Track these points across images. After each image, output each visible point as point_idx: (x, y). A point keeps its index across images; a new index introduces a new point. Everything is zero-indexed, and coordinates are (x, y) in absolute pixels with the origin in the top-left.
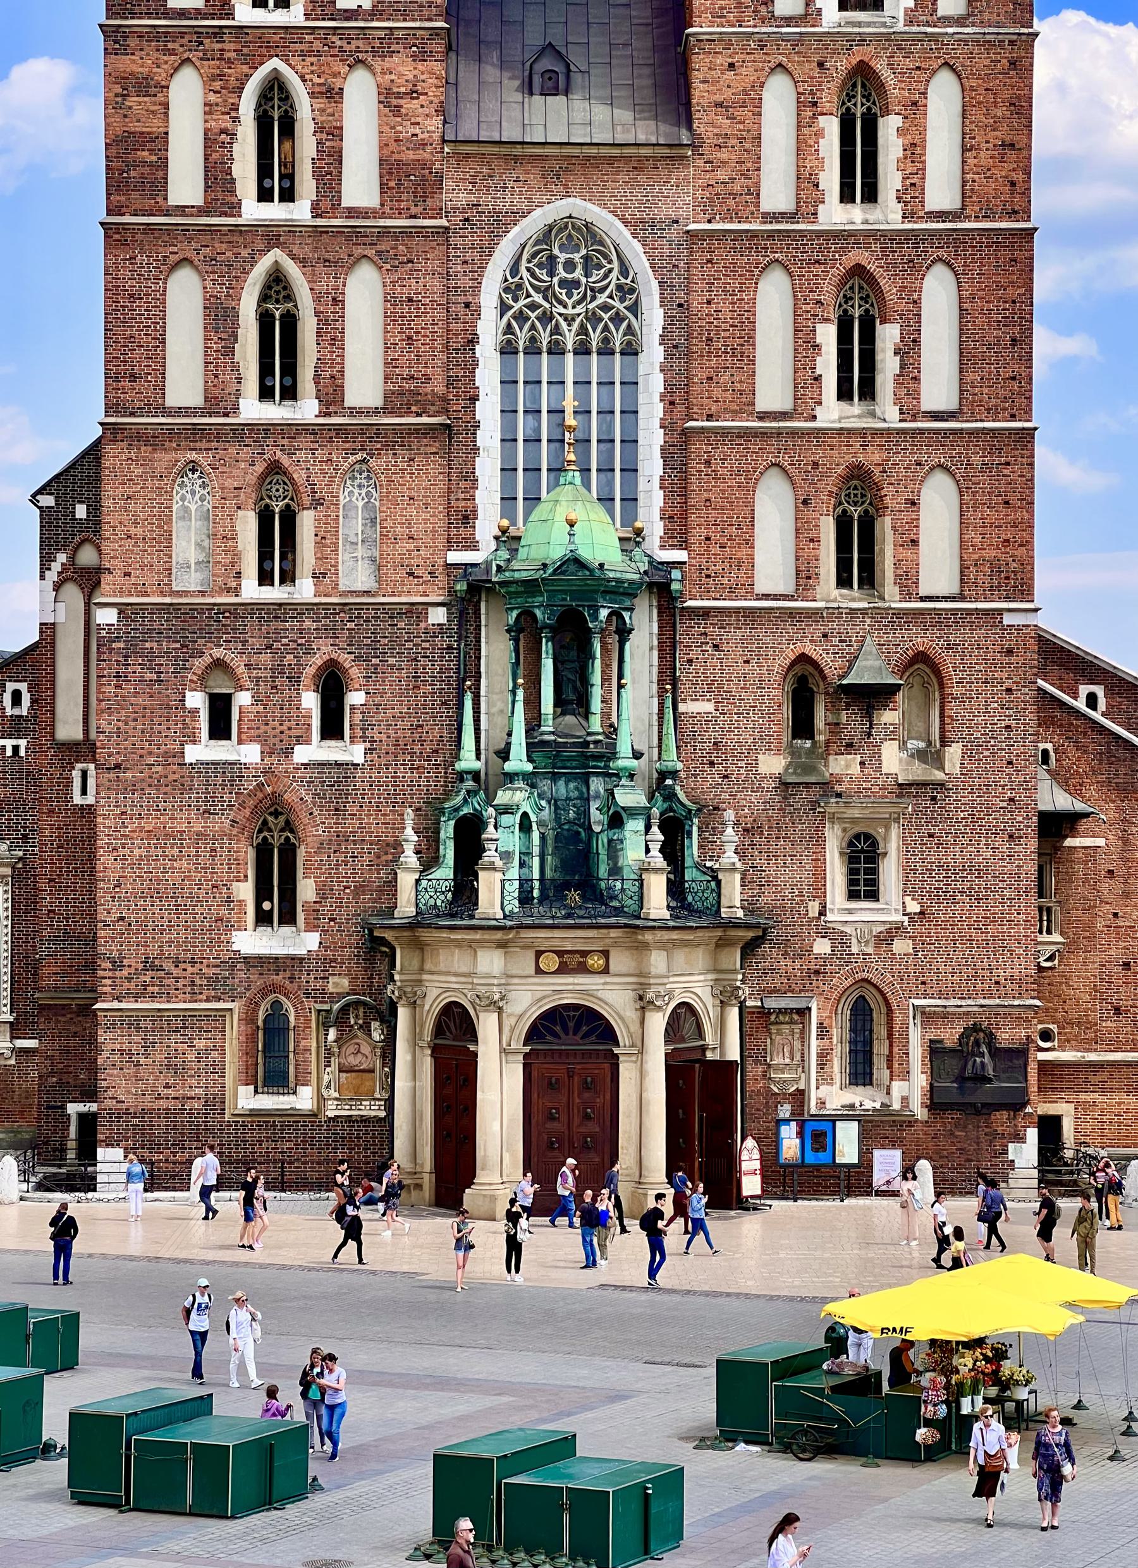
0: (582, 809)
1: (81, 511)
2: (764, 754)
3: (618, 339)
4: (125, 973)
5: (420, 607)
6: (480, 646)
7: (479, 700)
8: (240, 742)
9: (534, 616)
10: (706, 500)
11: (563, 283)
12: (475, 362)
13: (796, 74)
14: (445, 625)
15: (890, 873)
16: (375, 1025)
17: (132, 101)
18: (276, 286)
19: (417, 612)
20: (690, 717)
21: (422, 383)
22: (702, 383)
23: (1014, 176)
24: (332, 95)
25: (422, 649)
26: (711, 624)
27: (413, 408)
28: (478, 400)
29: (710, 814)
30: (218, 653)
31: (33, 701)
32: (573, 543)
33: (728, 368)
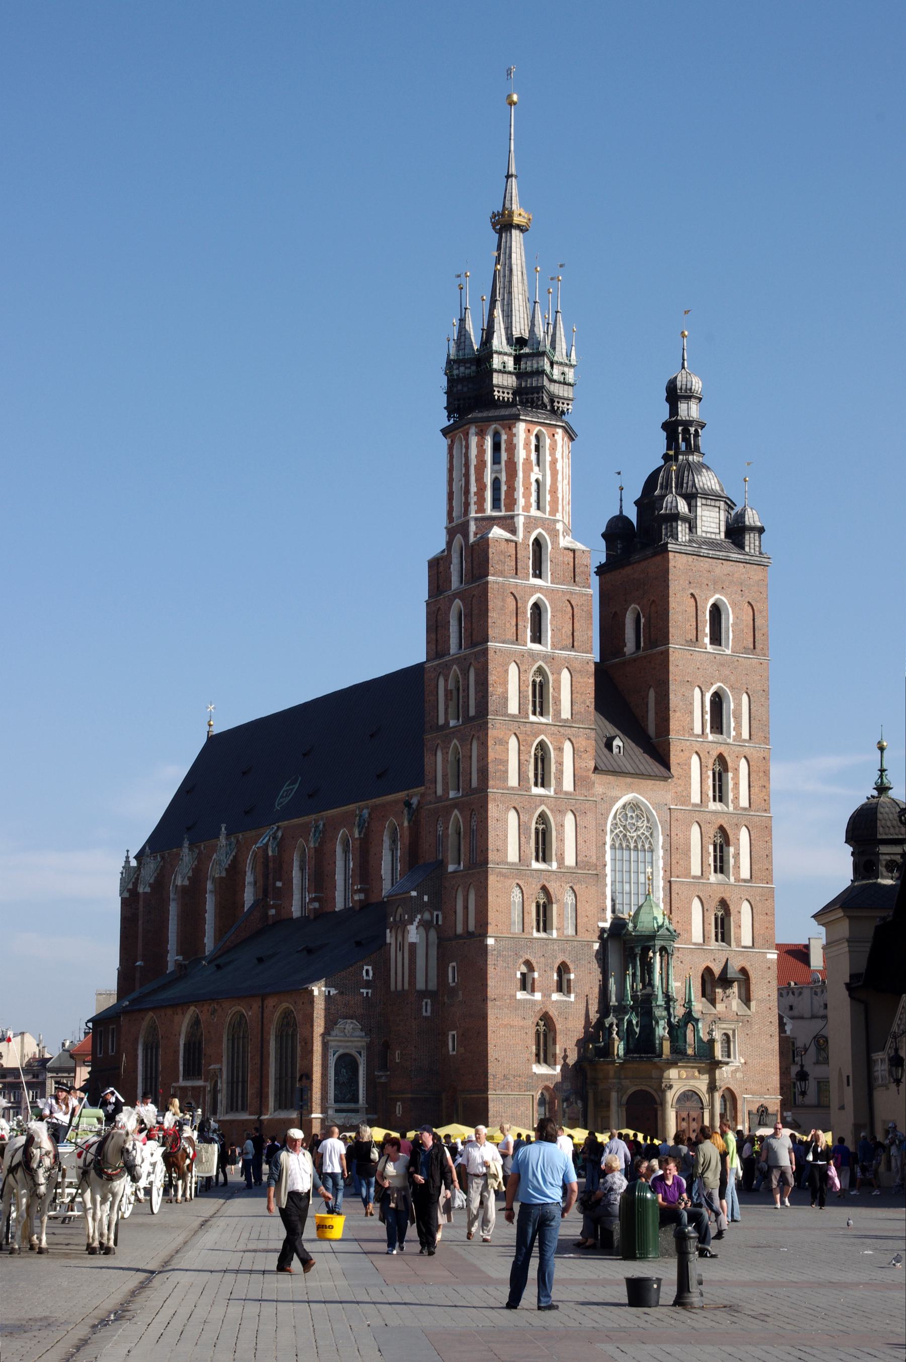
1: (426, 898)
3: (647, 846)
4: (497, 1080)
8: (533, 991)
11: (629, 823)
12: (605, 852)
13: (701, 756)
15: (736, 1047)
16: (579, 1102)
17: (497, 746)
18: (543, 818)
19: (589, 944)
23: (766, 798)
24: (560, 750)
30: (528, 957)
31: (374, 974)
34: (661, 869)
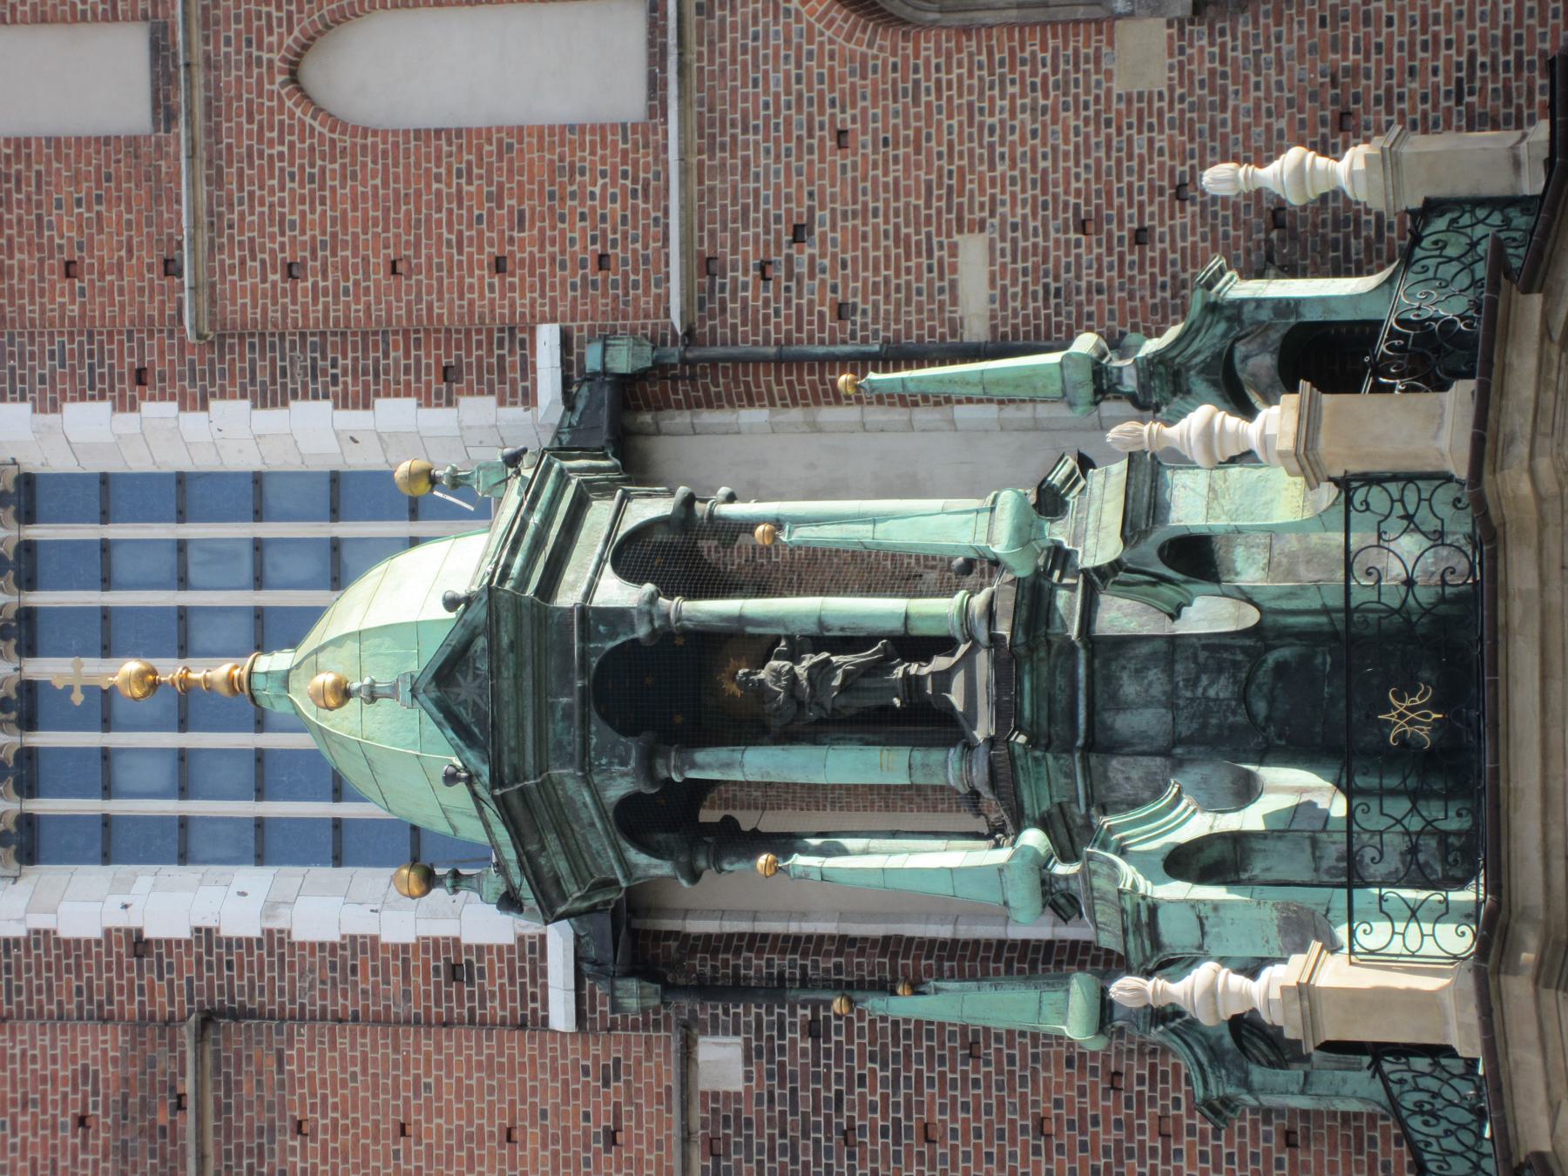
0: (1203, 655)
2: (1109, 74)
5: (697, 1114)
6: (809, 938)
7: (966, 943)
9: (628, 805)
10: (394, 271)
14: (747, 1041)
20: (1004, 306)
21: (96, 1093)
22: (82, 292)
25: (816, 1111)
26: (734, 251)
27: (163, 1118)
28: (140, 931)
29: (1294, 237)
32: (394, 687)
33: (39, 218)
34: (127, 422)
